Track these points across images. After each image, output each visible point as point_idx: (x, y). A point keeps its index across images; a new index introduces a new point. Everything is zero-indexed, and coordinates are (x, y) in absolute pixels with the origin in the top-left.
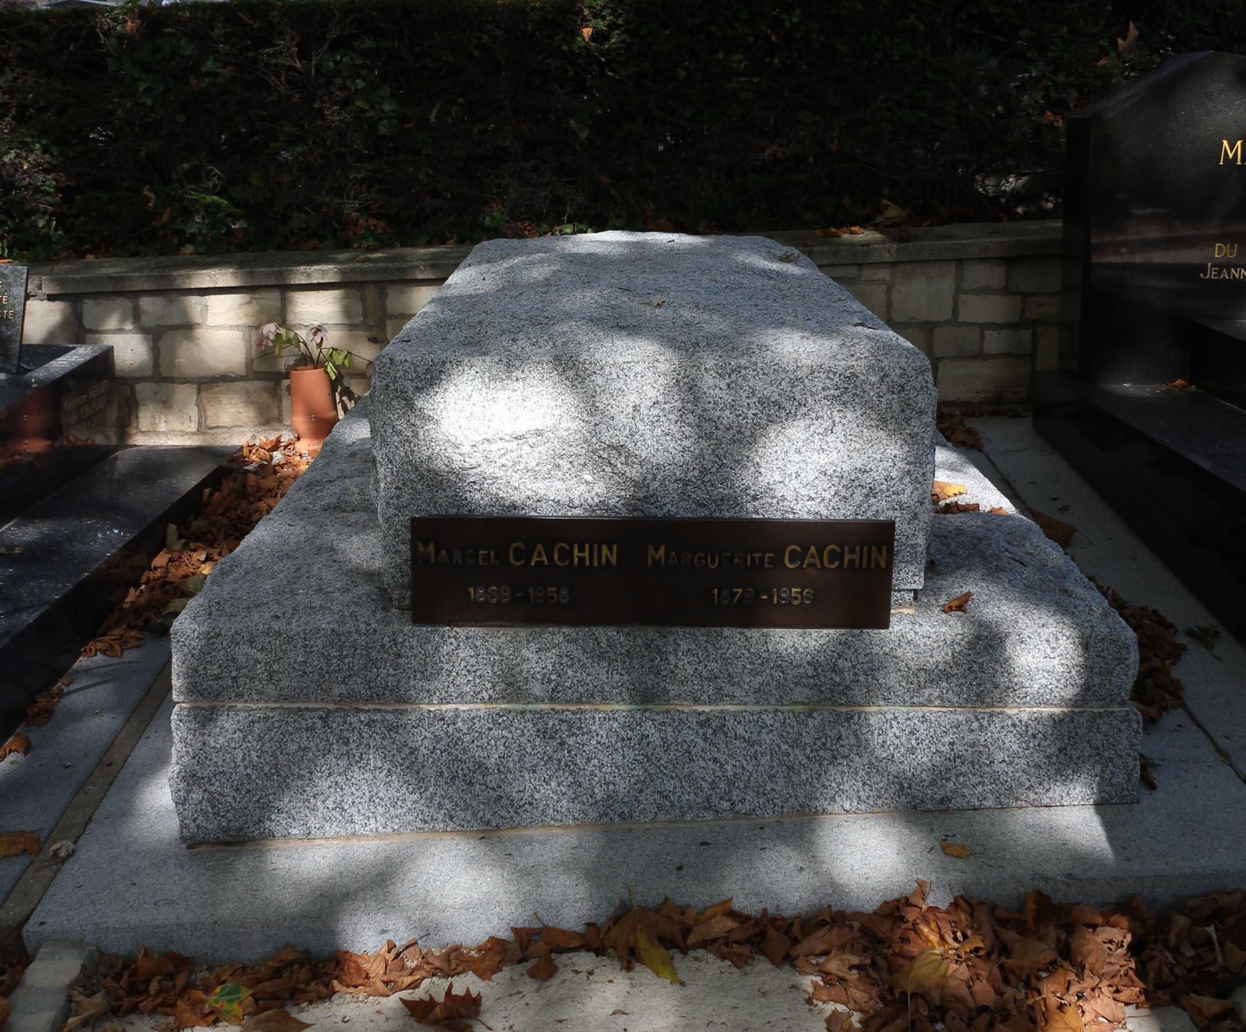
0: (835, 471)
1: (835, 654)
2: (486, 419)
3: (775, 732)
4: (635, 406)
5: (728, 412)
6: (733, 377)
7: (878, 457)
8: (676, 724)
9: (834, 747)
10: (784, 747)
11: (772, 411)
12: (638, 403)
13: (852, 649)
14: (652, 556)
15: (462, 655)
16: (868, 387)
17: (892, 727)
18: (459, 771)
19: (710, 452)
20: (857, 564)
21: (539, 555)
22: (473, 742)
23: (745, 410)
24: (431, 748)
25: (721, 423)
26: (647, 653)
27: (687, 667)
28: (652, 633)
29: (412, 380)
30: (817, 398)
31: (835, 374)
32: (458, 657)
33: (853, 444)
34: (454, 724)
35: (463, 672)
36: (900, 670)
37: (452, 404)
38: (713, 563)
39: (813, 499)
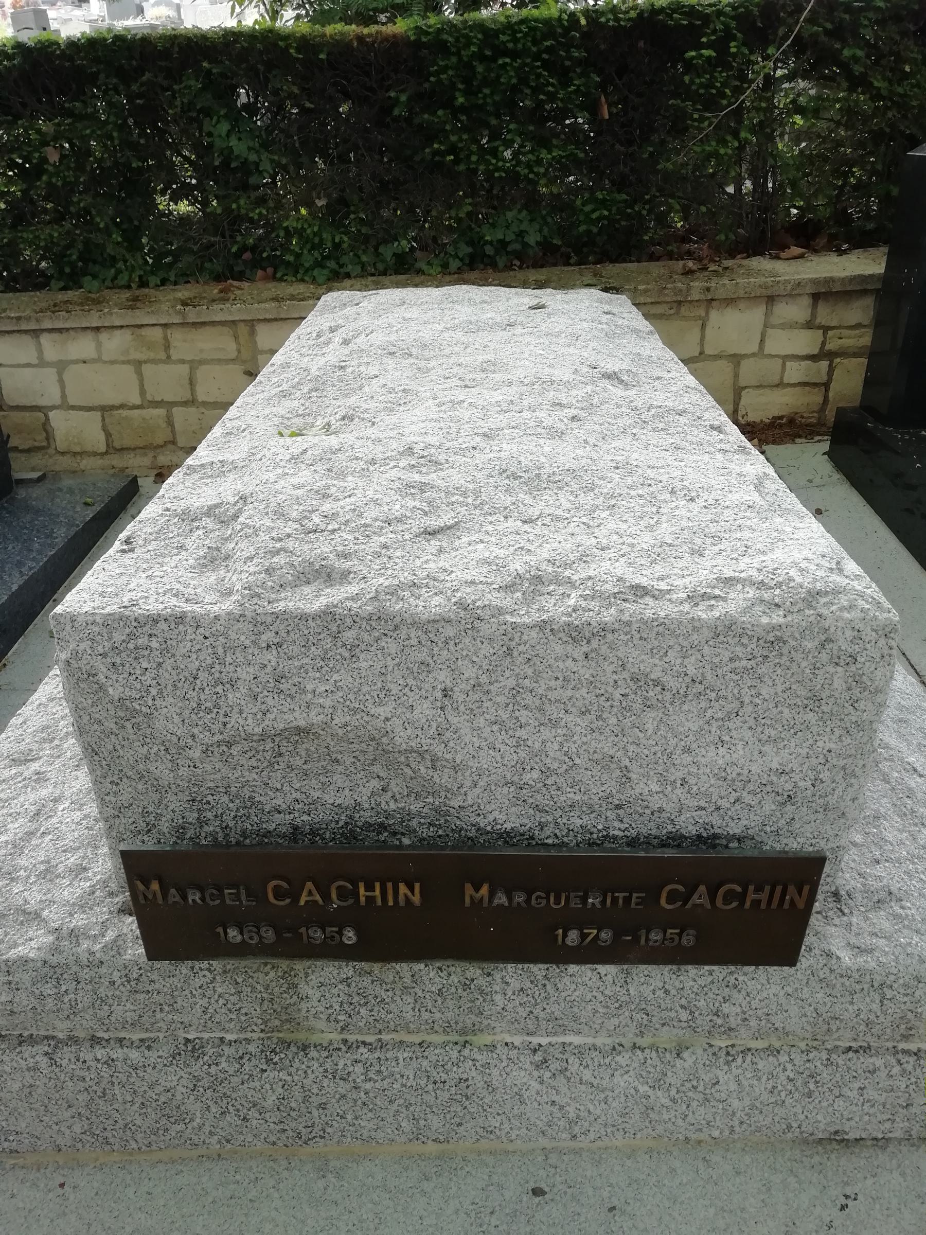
0: (739, 774)
1: (720, 998)
2: (222, 712)
3: (631, 1073)
4: (445, 690)
5: (584, 690)
6: (594, 643)
7: (804, 752)
8: (504, 1064)
9: (708, 1091)
10: (643, 1089)
11: (651, 693)
12: (449, 684)
13: (744, 993)
14: (471, 897)
15: (220, 990)
16: (798, 656)
17: (785, 1070)
18: (230, 1107)
19: (556, 747)
20: (763, 906)
21: (310, 893)
22: (243, 1083)
23: (610, 689)
24: (191, 1086)
25: (573, 705)
26: (465, 994)
27: (520, 1009)
28: (473, 971)
29: (104, 655)
30: (719, 672)
31: (750, 638)
32: (215, 991)
33: (767, 732)
34: (217, 1064)
35: (223, 1011)
36: (806, 1016)
37: (169, 687)
38: (557, 902)
39: (704, 809)
